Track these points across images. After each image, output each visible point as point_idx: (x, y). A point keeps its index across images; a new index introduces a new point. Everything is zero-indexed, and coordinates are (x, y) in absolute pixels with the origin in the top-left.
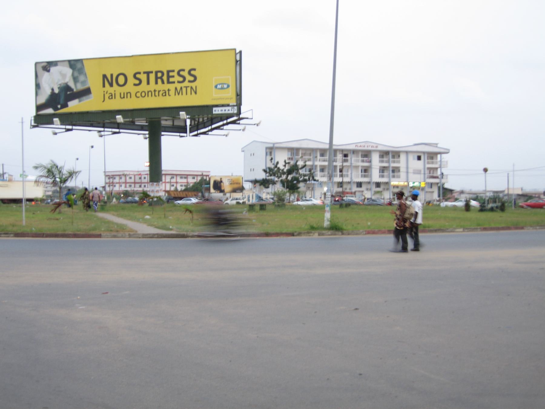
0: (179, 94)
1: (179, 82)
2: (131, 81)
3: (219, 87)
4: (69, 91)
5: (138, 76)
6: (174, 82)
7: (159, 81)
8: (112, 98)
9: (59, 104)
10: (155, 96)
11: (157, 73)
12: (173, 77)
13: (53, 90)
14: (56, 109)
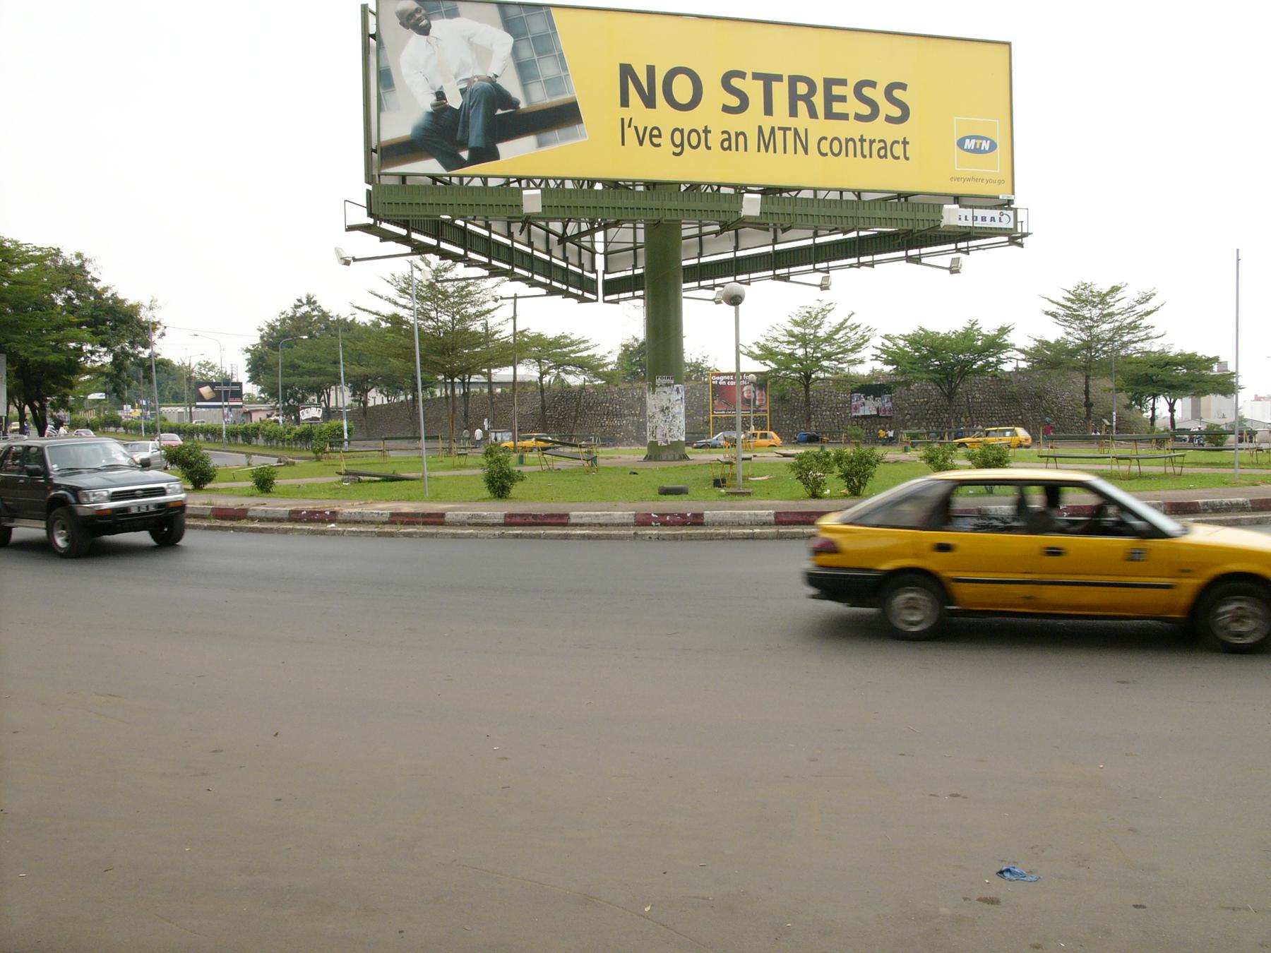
0: (767, 149)
1: (859, 117)
2: (715, 95)
3: (969, 144)
4: (502, 109)
5: (735, 82)
6: (844, 117)
7: (802, 106)
8: (729, 148)
9: (464, 145)
10: (864, 156)
11: (794, 80)
12: (843, 99)
13: (440, 95)
14: (452, 161)
